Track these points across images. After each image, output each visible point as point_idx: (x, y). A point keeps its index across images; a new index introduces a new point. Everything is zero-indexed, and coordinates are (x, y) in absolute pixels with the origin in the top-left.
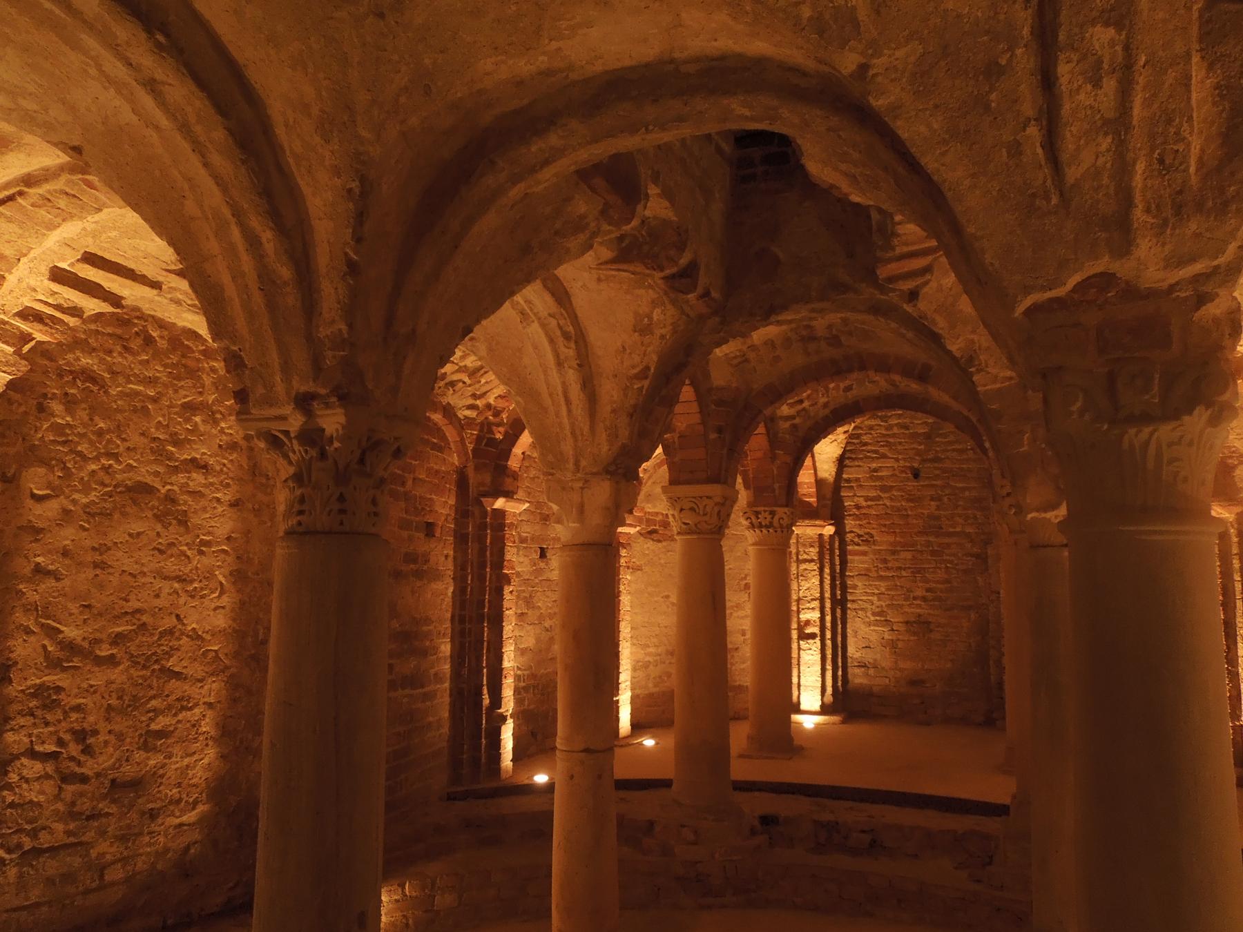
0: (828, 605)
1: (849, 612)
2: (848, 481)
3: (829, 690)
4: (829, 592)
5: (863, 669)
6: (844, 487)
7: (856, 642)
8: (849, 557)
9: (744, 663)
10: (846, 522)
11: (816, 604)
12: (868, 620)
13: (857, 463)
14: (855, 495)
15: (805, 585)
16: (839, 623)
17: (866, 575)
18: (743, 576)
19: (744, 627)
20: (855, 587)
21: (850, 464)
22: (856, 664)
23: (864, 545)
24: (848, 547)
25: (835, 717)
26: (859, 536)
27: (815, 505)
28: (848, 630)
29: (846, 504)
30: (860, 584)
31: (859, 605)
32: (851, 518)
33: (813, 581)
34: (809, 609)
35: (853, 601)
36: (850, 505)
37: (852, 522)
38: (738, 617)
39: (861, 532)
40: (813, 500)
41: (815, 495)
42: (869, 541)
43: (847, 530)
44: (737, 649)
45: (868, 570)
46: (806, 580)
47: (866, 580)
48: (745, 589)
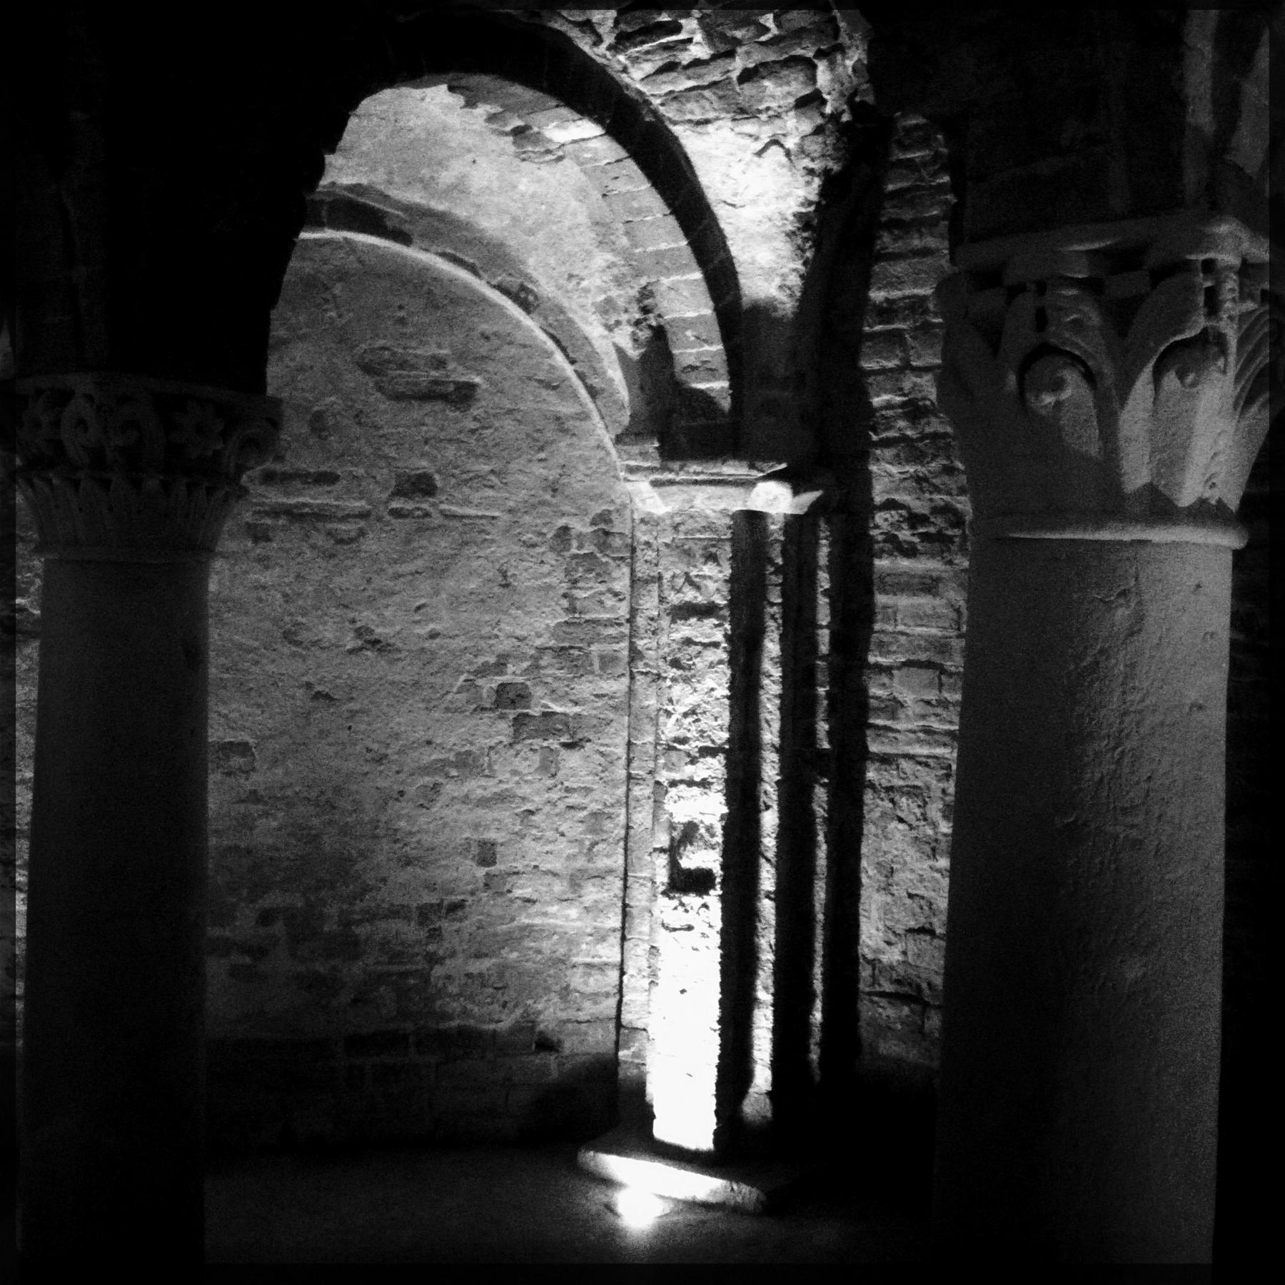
0: (770, 770)
1: (868, 797)
2: (887, 311)
3: (762, 1078)
4: (776, 726)
5: (906, 1010)
6: (873, 336)
7: (886, 910)
8: (881, 599)
9: (479, 956)
10: (873, 468)
11: (714, 768)
12: (930, 832)
13: (916, 243)
14: (906, 367)
15: (684, 696)
16: (821, 838)
17: (929, 665)
18: (492, 660)
19: (492, 835)
20: (893, 707)
21: (897, 247)
22: (888, 987)
23: (933, 556)
24: (877, 562)
25: (745, 1189)
26: (914, 520)
27: (726, 404)
28: (864, 863)
29: (877, 401)
30: (908, 697)
31: (903, 775)
32: (889, 453)
33: (709, 682)
34: (690, 783)
35: (886, 760)
36: (889, 406)
37: (894, 470)
38: (466, 799)
39: (920, 507)
40: (718, 386)
41: (720, 362)
42: (951, 539)
43: (878, 499)
44: (456, 907)
45: (941, 647)
46: (687, 680)
47: (930, 685)
48: (498, 704)
